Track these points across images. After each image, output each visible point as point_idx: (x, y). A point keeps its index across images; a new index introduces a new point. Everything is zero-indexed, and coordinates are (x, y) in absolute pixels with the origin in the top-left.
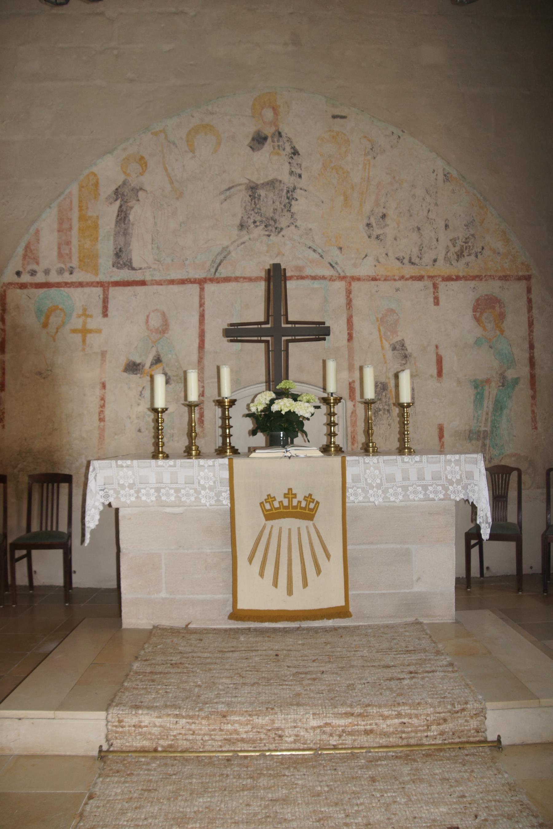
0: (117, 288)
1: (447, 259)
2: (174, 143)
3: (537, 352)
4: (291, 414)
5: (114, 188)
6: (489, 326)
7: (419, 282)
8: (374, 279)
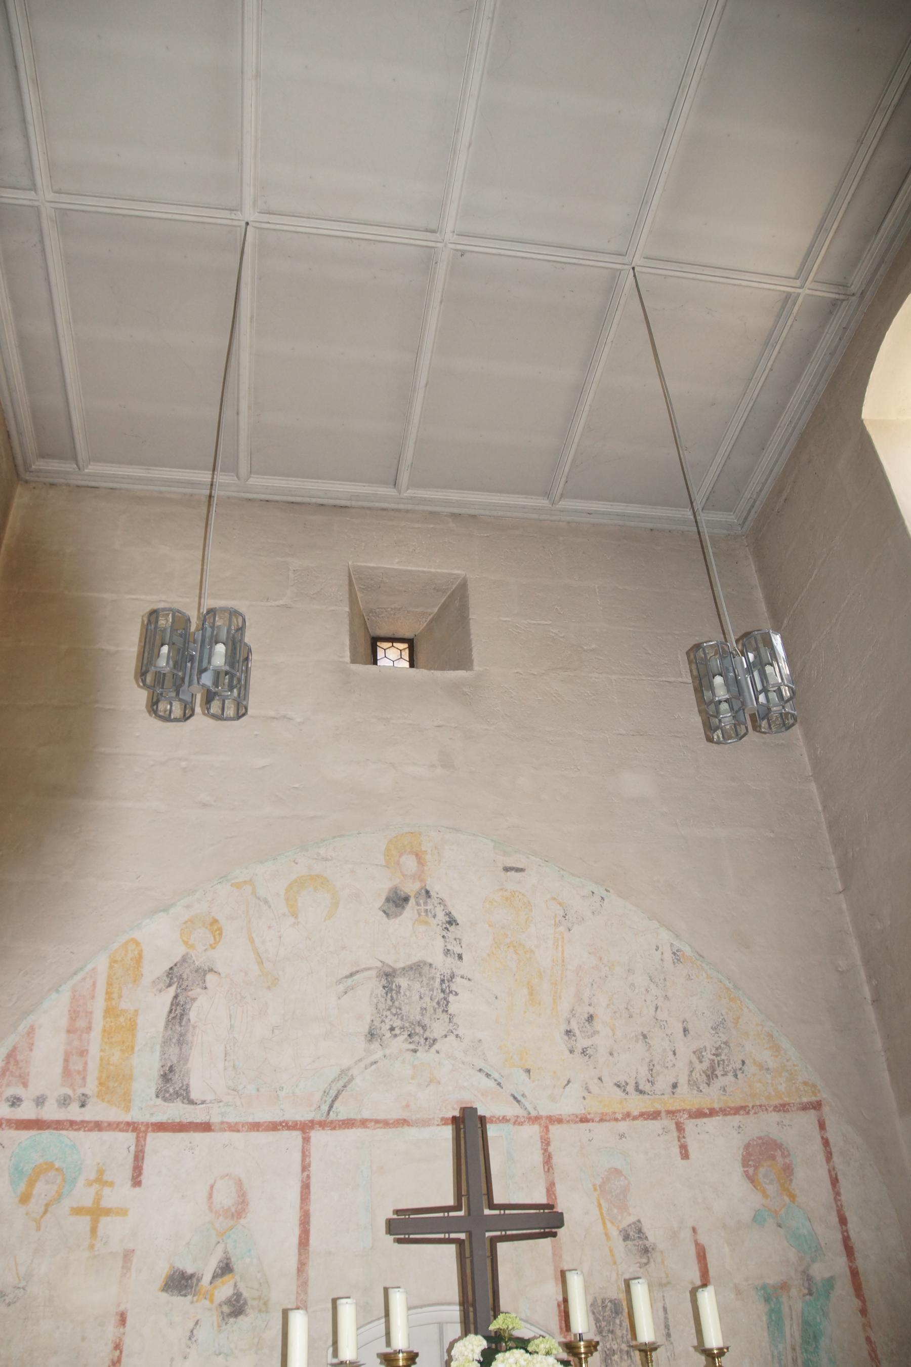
0: (161, 1134)
1: (692, 1083)
2: (266, 902)
6: (772, 1189)
7: (654, 1122)
8: (584, 1120)
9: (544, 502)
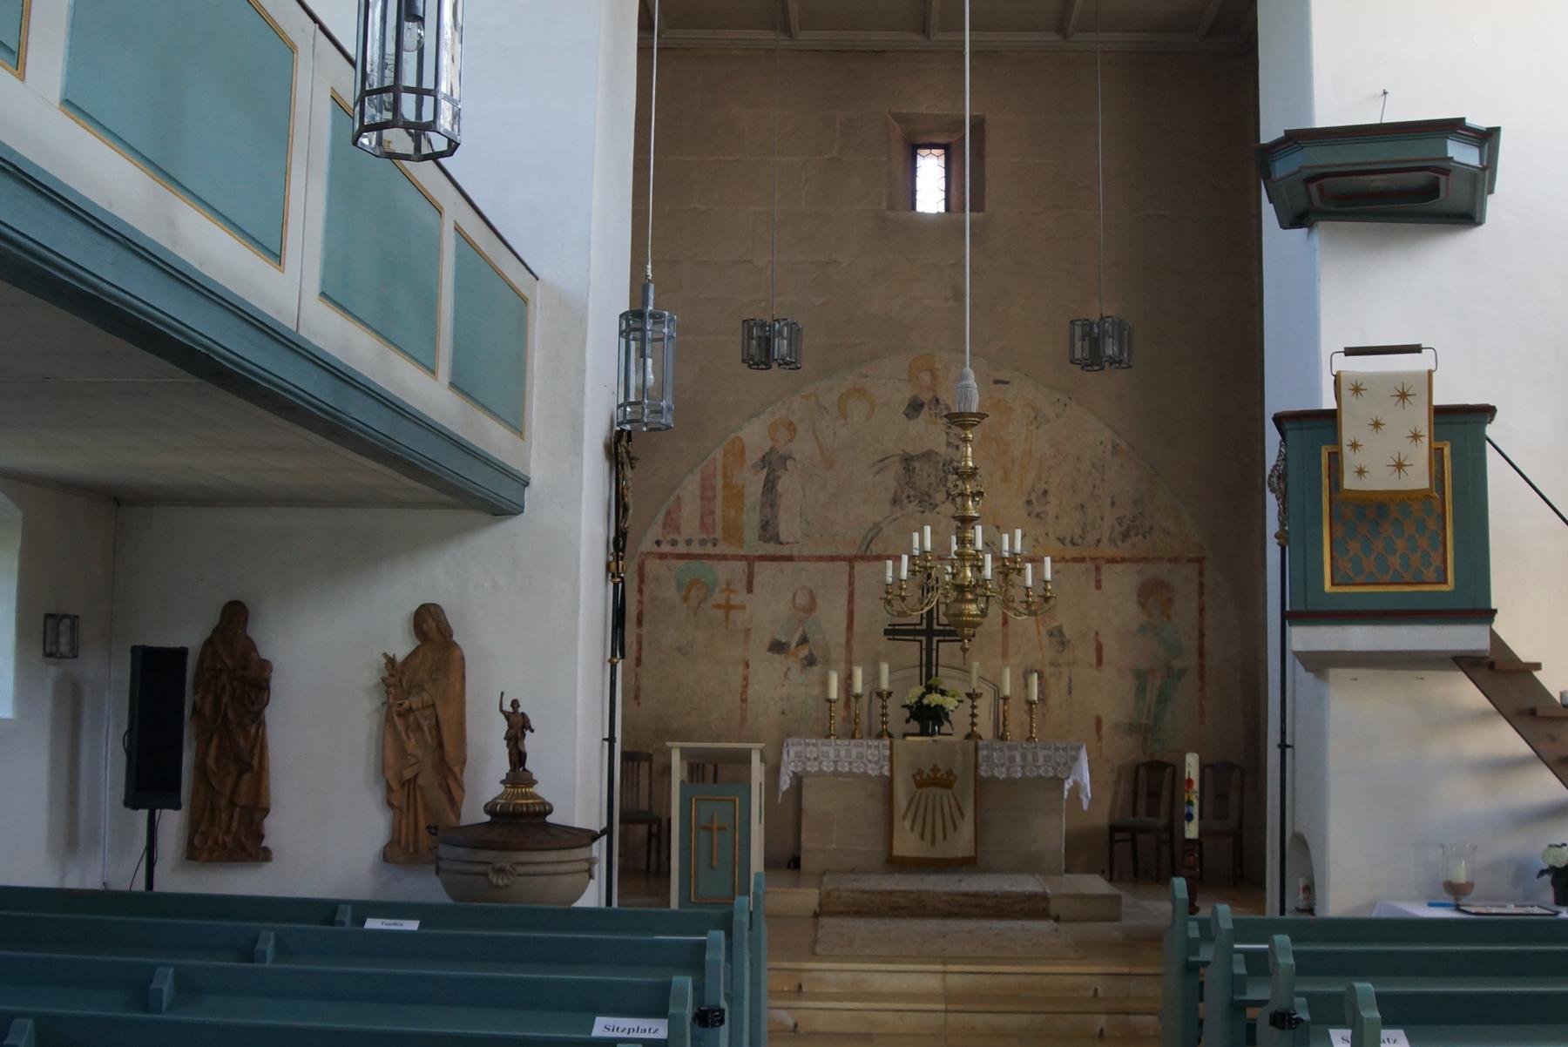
1: (1112, 540)
4: (940, 708)
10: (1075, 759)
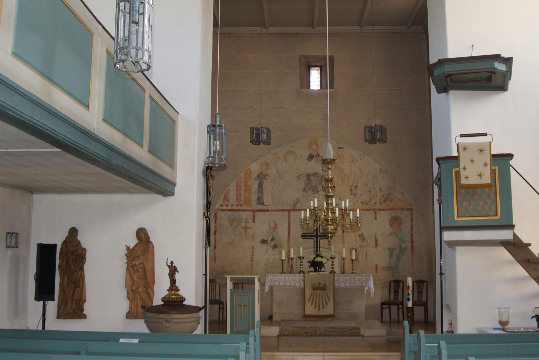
1: (380, 203)
3: (414, 238)
4: (321, 262)
5: (257, 175)
9: (358, 28)
10: (368, 280)
